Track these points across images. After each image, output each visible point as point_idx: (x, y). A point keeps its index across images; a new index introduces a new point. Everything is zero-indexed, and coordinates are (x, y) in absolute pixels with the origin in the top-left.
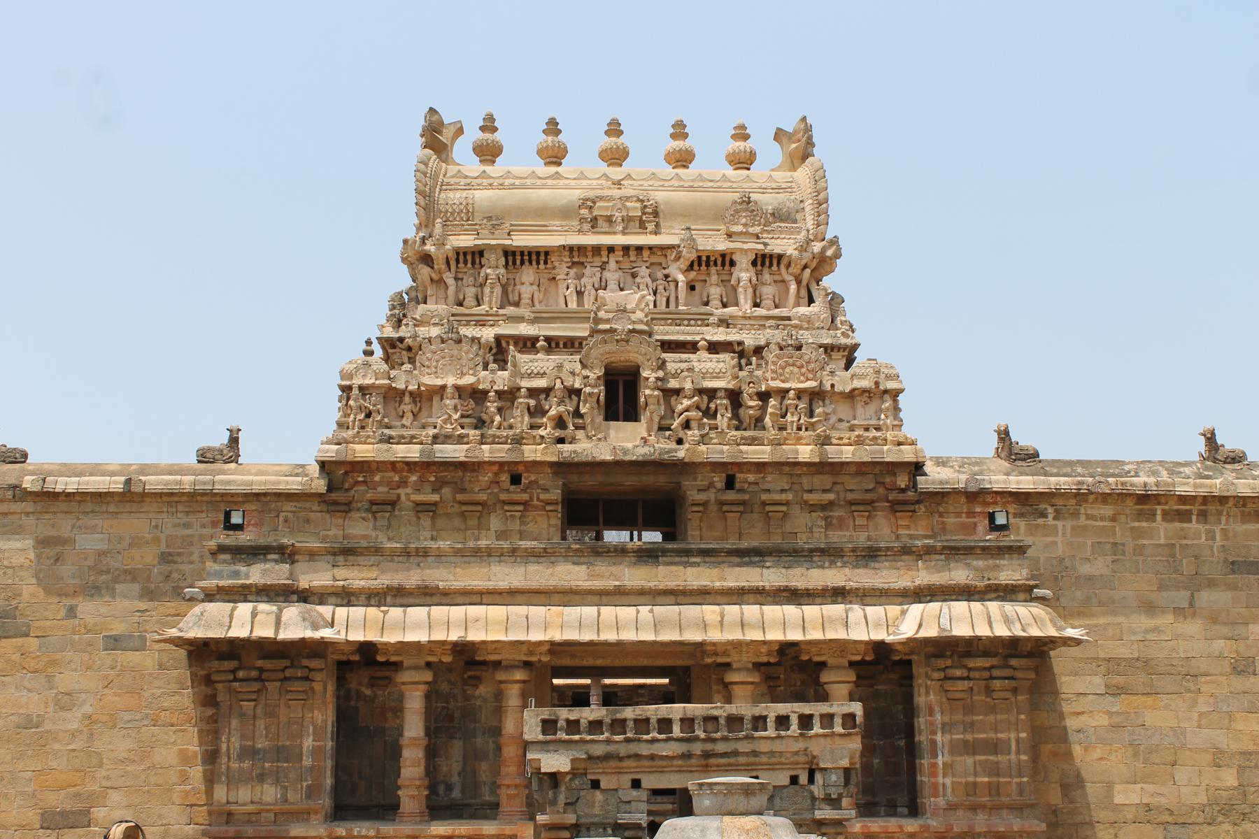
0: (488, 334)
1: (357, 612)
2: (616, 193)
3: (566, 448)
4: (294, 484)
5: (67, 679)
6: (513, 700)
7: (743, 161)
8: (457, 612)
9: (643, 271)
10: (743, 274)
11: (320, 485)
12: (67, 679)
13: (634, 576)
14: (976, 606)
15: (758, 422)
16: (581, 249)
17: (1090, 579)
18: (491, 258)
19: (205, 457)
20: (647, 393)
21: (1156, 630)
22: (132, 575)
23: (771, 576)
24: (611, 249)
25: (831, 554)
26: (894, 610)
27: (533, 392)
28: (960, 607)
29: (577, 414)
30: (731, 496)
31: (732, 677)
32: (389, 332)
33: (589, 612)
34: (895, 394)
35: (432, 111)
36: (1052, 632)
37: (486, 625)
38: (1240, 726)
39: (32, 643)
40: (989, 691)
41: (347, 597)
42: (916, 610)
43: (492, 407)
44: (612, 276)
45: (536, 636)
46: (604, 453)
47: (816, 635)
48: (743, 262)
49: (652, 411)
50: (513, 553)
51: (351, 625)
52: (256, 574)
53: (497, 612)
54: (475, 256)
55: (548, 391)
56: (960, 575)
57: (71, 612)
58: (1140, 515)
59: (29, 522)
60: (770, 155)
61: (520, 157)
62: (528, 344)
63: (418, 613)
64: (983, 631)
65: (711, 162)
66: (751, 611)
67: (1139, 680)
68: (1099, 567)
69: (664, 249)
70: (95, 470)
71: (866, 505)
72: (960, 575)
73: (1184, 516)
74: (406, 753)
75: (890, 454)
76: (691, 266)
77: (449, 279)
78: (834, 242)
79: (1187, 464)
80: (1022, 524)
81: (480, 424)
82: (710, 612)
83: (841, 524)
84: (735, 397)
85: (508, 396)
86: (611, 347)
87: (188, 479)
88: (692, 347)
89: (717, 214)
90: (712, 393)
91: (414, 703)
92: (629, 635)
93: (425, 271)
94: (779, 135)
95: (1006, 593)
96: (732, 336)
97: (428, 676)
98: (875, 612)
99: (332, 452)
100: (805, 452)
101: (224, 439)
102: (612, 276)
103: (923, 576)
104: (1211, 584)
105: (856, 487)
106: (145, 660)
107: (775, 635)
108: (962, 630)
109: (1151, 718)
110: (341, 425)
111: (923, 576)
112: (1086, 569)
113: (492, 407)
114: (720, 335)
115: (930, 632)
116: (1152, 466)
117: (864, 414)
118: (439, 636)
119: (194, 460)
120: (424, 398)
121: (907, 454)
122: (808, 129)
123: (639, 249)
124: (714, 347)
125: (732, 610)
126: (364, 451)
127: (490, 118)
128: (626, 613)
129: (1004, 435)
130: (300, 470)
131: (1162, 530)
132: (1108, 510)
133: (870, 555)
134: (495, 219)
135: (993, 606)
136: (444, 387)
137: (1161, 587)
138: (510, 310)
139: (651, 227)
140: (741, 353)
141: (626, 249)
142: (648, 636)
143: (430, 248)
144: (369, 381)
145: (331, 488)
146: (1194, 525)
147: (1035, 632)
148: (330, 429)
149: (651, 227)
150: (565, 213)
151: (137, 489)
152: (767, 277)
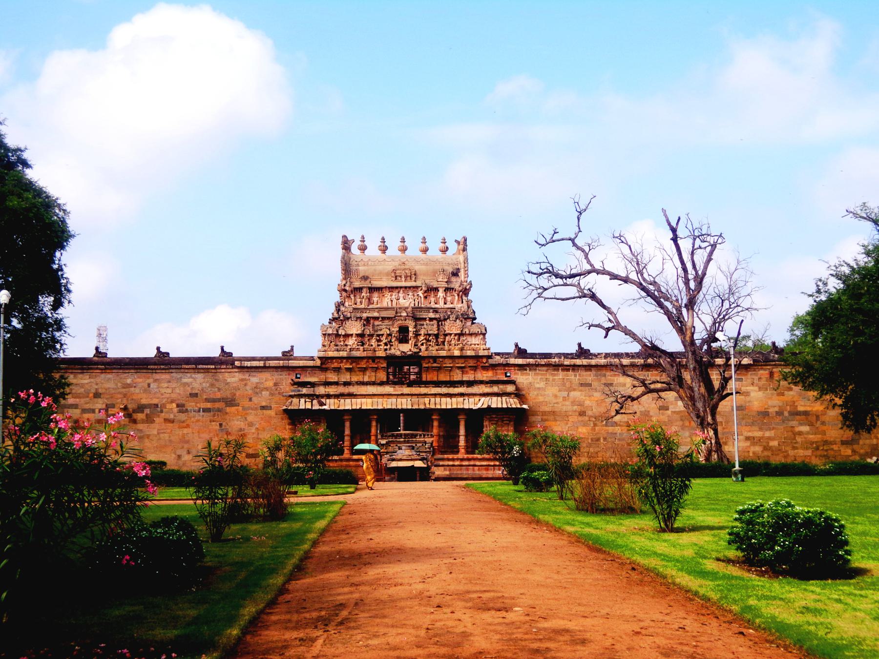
0: (365, 315)
1: (332, 401)
2: (403, 267)
3: (388, 352)
4: (311, 363)
5: (250, 418)
6: (374, 424)
7: (445, 250)
8: (359, 400)
9: (411, 294)
10: (441, 294)
11: (318, 363)
12: (250, 418)
13: (406, 390)
14: (499, 398)
15: (443, 343)
16: (392, 288)
17: (539, 389)
18: (365, 290)
19: (284, 353)
20: (411, 334)
21: (557, 403)
22: (267, 389)
23: (444, 390)
24: (401, 287)
25: (461, 383)
26: (477, 399)
27: (378, 335)
28: (495, 399)
29: (391, 341)
30: (435, 365)
31: (434, 417)
32: (336, 315)
33: (394, 400)
34: (484, 335)
35: (344, 237)
36: (519, 406)
37: (367, 404)
38: (580, 430)
39: (240, 408)
40: (503, 421)
41: (329, 396)
42: (483, 399)
43: (366, 339)
44: (401, 295)
45: (380, 407)
46: (398, 353)
47: (455, 406)
48: (441, 290)
49: (412, 341)
50: (373, 384)
51: (330, 405)
52: (304, 391)
53: (369, 401)
54: (360, 289)
55: (382, 335)
56: (495, 389)
57: (250, 399)
58: (555, 370)
59: (237, 374)
60: (453, 248)
61: (373, 250)
62: (376, 318)
63: (348, 401)
64: (500, 406)
65: (434, 252)
66: (438, 399)
67: (552, 418)
68: (542, 385)
69: (417, 287)
70: (253, 359)
71: (475, 369)
72: (495, 389)
73: (568, 370)
74: (346, 438)
75: (481, 353)
76: (425, 292)
77: (352, 296)
78: (471, 284)
79: (572, 354)
80: (519, 372)
81: (363, 345)
82: (427, 400)
83: (467, 373)
84: (437, 336)
85: (371, 336)
86: (400, 322)
87: (281, 362)
88: (425, 319)
89: (434, 273)
90: (430, 335)
91: (347, 424)
92: (404, 407)
93: (344, 294)
94: (458, 242)
95: (508, 394)
96: (437, 316)
97: (350, 417)
98: (471, 400)
99: (322, 354)
100: (457, 353)
101: (289, 349)
102: (401, 295)
103: (487, 390)
104: (574, 390)
105: (472, 363)
106: (271, 413)
107: (443, 407)
108: (494, 406)
109: (556, 429)
110: (324, 346)
111: (487, 390)
112: (537, 386)
113: (366, 339)
114: (432, 315)
115: (485, 406)
116: (559, 355)
117: (474, 340)
118: (354, 407)
119: (280, 355)
120: (347, 336)
121: (486, 353)
122: (465, 240)
123: (410, 287)
124: (431, 319)
125: (433, 400)
126: (331, 354)
127: (363, 237)
128: (404, 400)
129: (517, 345)
130: (312, 359)
131: (561, 374)
132: (545, 368)
133: (470, 384)
134: (365, 278)
135: (504, 398)
136: (352, 335)
137: (560, 391)
138: (371, 306)
139: (413, 279)
140: (439, 320)
141: (406, 287)
142: (409, 407)
143: (347, 288)
144: (331, 332)
145: (322, 364)
146: (571, 373)
147: (514, 406)
148: (320, 347)
149: (413, 279)
150: (387, 274)
151: (267, 365)
152: (448, 294)
